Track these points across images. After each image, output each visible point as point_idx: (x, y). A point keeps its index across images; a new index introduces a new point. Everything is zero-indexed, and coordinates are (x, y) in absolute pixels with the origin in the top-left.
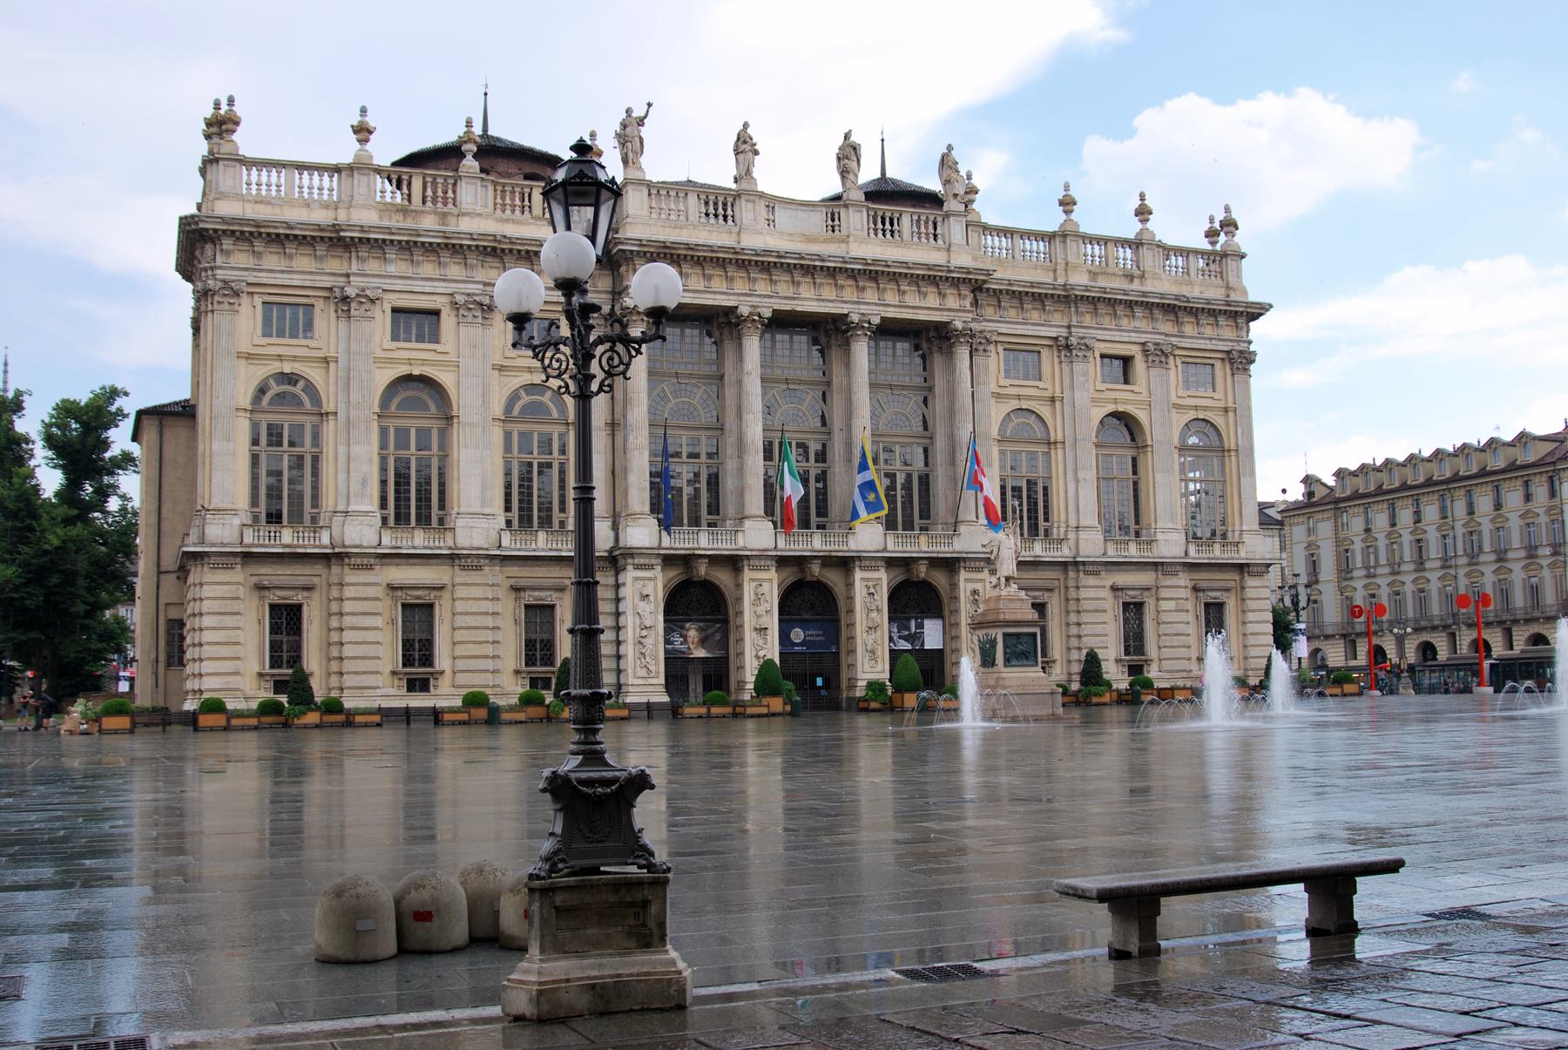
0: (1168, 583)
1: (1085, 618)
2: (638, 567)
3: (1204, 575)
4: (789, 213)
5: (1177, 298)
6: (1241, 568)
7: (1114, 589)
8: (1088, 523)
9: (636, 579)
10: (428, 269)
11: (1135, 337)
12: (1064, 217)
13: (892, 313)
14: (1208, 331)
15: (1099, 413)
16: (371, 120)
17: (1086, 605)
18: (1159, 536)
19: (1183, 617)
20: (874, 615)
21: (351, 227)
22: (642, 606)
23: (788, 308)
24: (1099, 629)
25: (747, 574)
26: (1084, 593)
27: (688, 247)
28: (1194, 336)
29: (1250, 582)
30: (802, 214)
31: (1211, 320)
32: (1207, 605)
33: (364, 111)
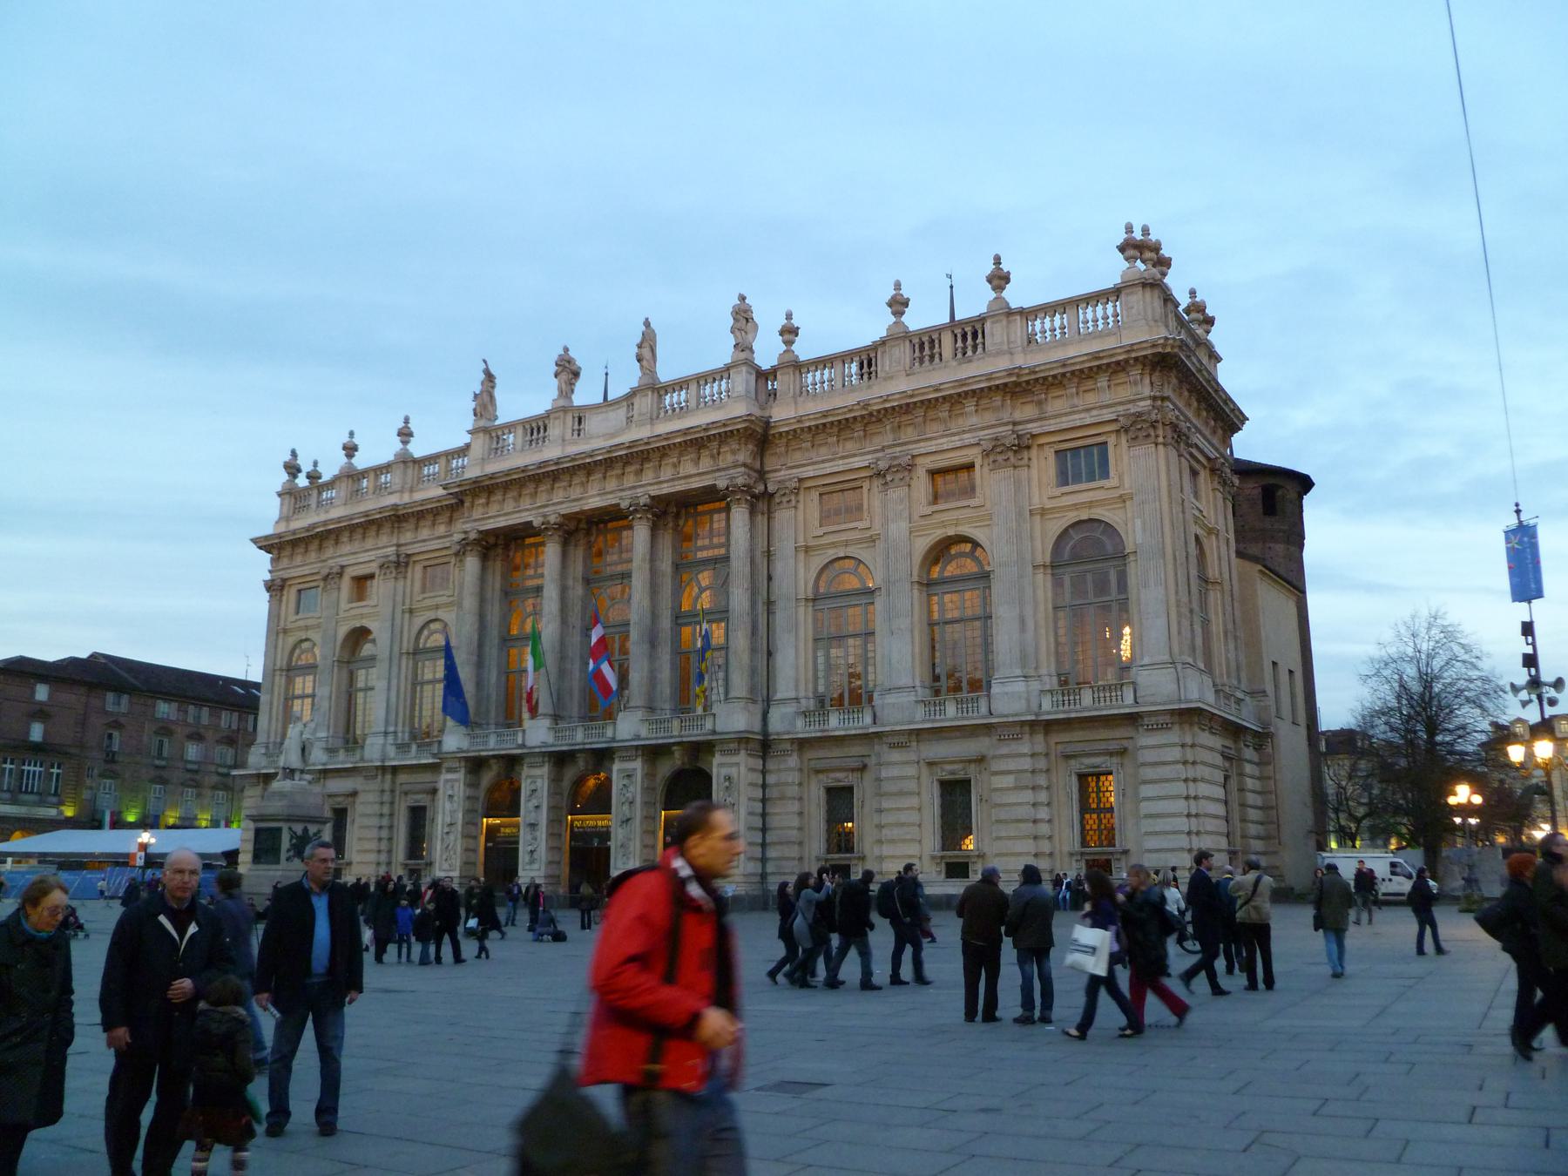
0: (1005, 750)
2: (450, 770)
3: (1078, 735)
4: (600, 417)
5: (1010, 372)
6: (1133, 719)
7: (930, 764)
9: (447, 781)
10: (369, 543)
11: (969, 438)
12: (893, 319)
13: (666, 489)
14: (1091, 399)
15: (922, 544)
16: (356, 440)
17: (888, 787)
18: (996, 689)
19: (1028, 796)
20: (626, 807)
21: (313, 526)
22: (448, 805)
23: (577, 509)
24: (903, 817)
27: (492, 476)
28: (1068, 413)
29: (1146, 740)
31: (1089, 384)
33: (352, 434)
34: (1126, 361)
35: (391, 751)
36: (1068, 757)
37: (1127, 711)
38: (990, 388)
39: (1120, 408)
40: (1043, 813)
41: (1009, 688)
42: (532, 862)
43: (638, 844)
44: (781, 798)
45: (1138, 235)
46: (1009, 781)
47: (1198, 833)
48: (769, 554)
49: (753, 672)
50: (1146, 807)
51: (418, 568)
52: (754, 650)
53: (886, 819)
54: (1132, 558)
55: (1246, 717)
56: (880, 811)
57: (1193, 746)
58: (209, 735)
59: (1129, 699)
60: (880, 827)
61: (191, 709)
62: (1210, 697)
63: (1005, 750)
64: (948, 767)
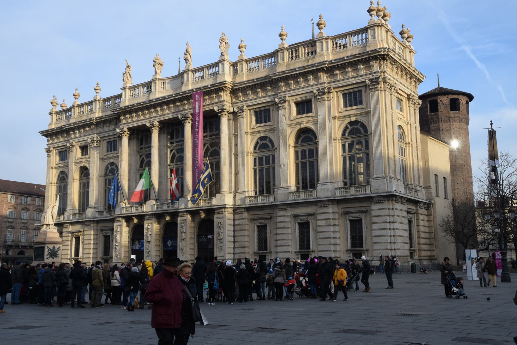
1: (279, 231)
6: (370, 199)
7: (295, 216)
8: (284, 186)
9: (117, 225)
17: (279, 225)
18: (319, 187)
19: (332, 229)
20: (183, 234)
23: (163, 119)
24: (285, 237)
25: (145, 222)
26: (279, 220)
29: (374, 207)
30: (176, 81)
32: (351, 221)
34: (369, 58)
35: (97, 215)
36: (345, 213)
37: (367, 196)
38: (316, 69)
39: (367, 76)
40: (337, 235)
41: (323, 187)
42: (149, 256)
43: (188, 249)
44: (240, 230)
45: (374, 6)
46: (323, 223)
47: (394, 243)
48: (236, 136)
49: (230, 181)
50: (375, 233)
51: (105, 142)
52: (230, 173)
53: (279, 237)
54: (370, 136)
55: (422, 196)
56: (276, 234)
57: (393, 209)
58: (31, 208)
59: (368, 191)
60: (276, 240)
61: (23, 198)
62: (403, 191)
63: (322, 211)
64: (301, 218)
